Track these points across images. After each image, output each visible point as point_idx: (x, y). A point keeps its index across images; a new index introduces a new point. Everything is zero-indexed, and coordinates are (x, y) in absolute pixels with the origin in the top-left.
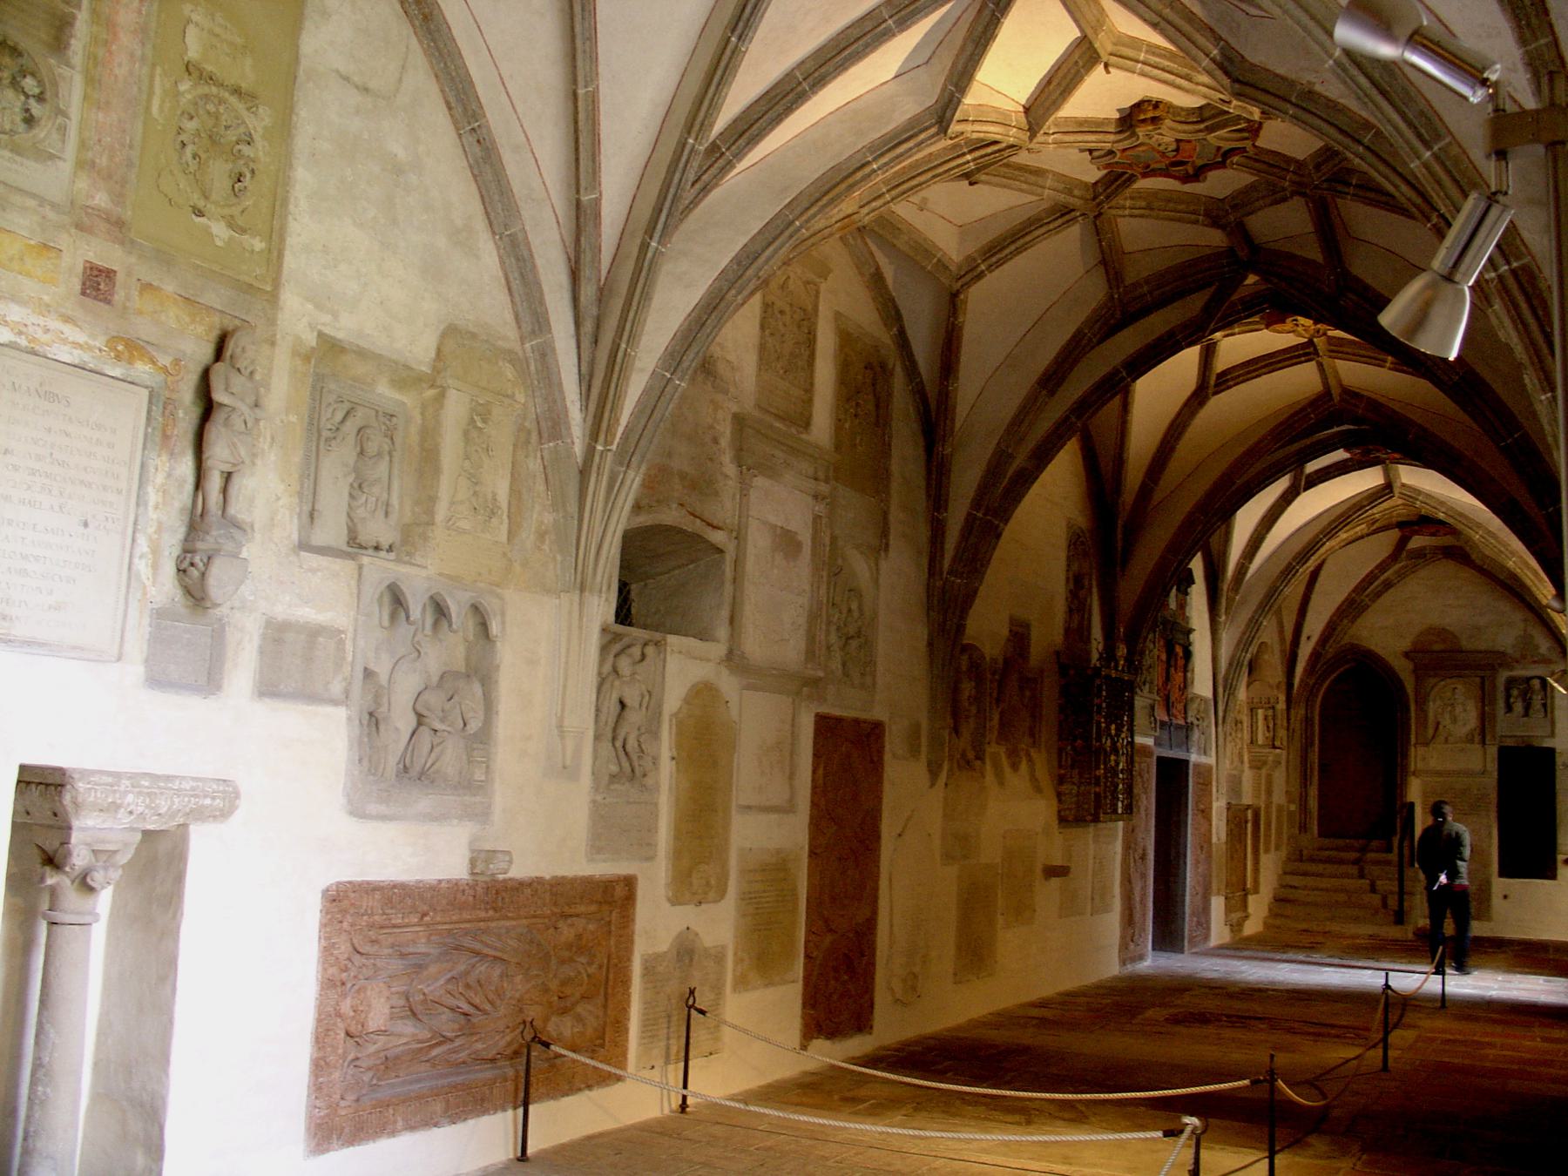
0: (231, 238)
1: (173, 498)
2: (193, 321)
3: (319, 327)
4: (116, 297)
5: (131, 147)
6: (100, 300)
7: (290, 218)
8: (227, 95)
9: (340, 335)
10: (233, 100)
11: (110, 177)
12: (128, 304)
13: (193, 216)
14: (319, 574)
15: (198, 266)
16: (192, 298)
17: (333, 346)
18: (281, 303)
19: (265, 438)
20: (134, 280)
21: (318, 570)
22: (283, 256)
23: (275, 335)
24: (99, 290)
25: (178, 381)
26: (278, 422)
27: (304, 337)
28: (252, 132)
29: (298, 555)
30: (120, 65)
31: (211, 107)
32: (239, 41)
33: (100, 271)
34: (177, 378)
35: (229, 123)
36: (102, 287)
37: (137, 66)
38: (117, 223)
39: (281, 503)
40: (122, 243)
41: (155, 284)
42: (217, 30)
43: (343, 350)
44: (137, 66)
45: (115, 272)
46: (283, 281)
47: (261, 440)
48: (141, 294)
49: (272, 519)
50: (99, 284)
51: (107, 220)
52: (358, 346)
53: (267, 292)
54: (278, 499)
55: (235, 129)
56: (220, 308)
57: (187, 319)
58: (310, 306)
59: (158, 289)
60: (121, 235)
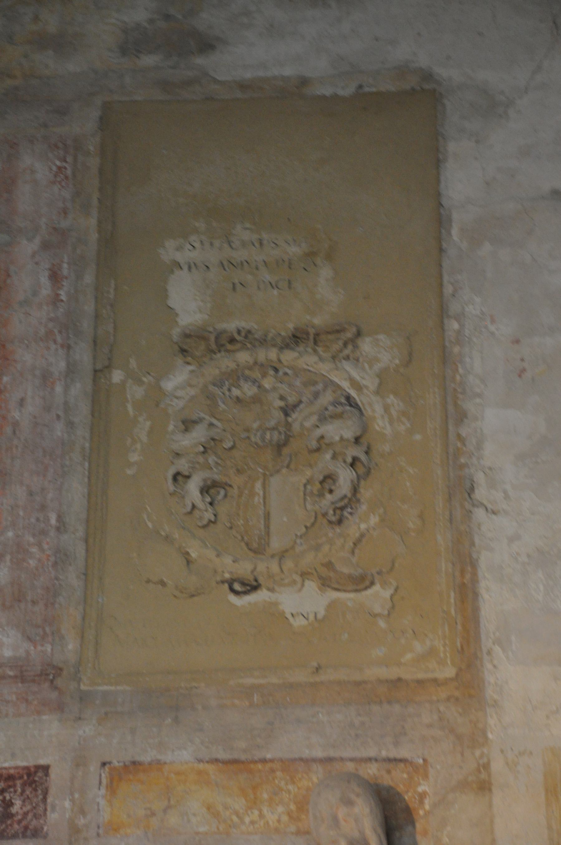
0: (332, 606)
4: (53, 817)
5: (61, 528)
6: (15, 836)
7: (479, 514)
8: (273, 354)
10: (288, 356)
11: (19, 598)
12: (81, 821)
13: (232, 598)
16: (243, 757)
18: (490, 693)
20: (94, 767)
22: (476, 595)
23: (487, 766)
24: (11, 816)
28: (353, 393)
30: (22, 402)
31: (249, 390)
32: (294, 250)
33: (10, 778)
35: (292, 400)
36: (17, 807)
37: (59, 389)
38: (43, 674)
40: (60, 708)
41: (146, 758)
42: (240, 255)
44: (59, 389)
45: (46, 769)
46: (486, 643)
48: (112, 789)
50: (10, 804)
51: (21, 678)
53: (446, 682)
55: (311, 403)
56: (319, 753)
57: (239, 804)
59: (158, 765)
60: (54, 695)
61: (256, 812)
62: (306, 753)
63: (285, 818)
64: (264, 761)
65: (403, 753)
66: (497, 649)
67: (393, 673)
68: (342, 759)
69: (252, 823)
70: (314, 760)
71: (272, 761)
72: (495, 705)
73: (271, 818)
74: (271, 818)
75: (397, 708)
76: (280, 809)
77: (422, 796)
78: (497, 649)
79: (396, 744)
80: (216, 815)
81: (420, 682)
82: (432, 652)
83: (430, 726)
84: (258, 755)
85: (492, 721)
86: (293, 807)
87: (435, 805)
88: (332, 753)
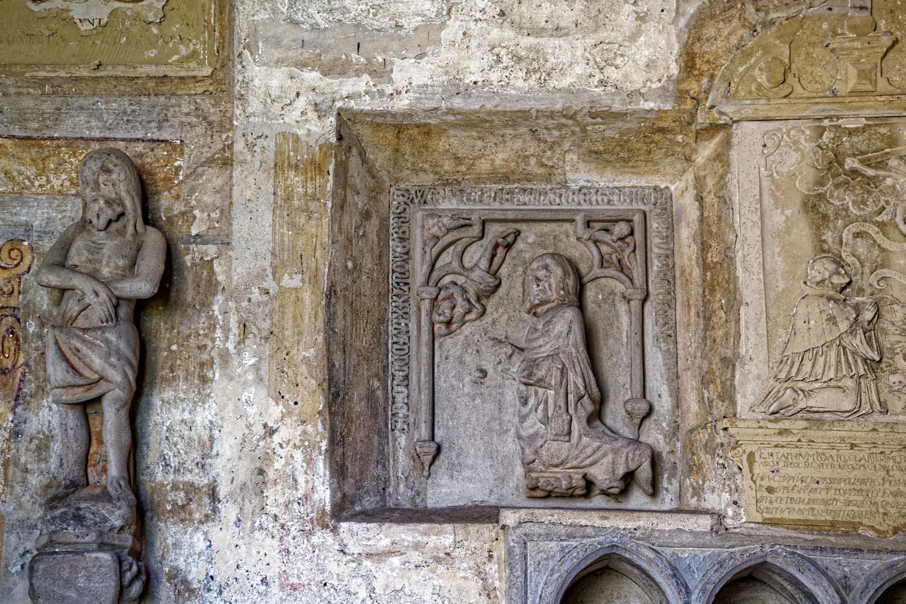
1: (26, 471)
2: (42, 172)
3: (339, 104)
9: (402, 104)
14: (396, 561)
15: (46, 79)
16: (35, 135)
17: (400, 129)
19: (226, 330)
21: (391, 553)
23: (230, 147)
25: (19, 276)
26: (256, 295)
27: (301, 132)
29: (335, 530)
34: (14, 272)
39: (277, 438)
43: (427, 131)
47: (219, 333)
49: (261, 472)
52: (450, 111)
54: (271, 432)
56: (97, 134)
57: (31, 172)
58: (312, 77)
61: (45, 178)
62: (87, 134)
63: (67, 183)
64: (52, 139)
65: (165, 135)
66: (246, 52)
67: (161, 71)
68: (115, 139)
69: (41, 186)
70: (93, 139)
71: (58, 139)
72: (241, 97)
73: (56, 183)
74: (56, 183)
75: (162, 99)
76: (64, 176)
77: (178, 169)
78: (246, 52)
79: (160, 128)
80: (12, 179)
81: (182, 78)
82: (194, 53)
83: (187, 114)
84: (48, 134)
85: (237, 112)
86: (74, 175)
87: (187, 176)
88: (107, 134)
